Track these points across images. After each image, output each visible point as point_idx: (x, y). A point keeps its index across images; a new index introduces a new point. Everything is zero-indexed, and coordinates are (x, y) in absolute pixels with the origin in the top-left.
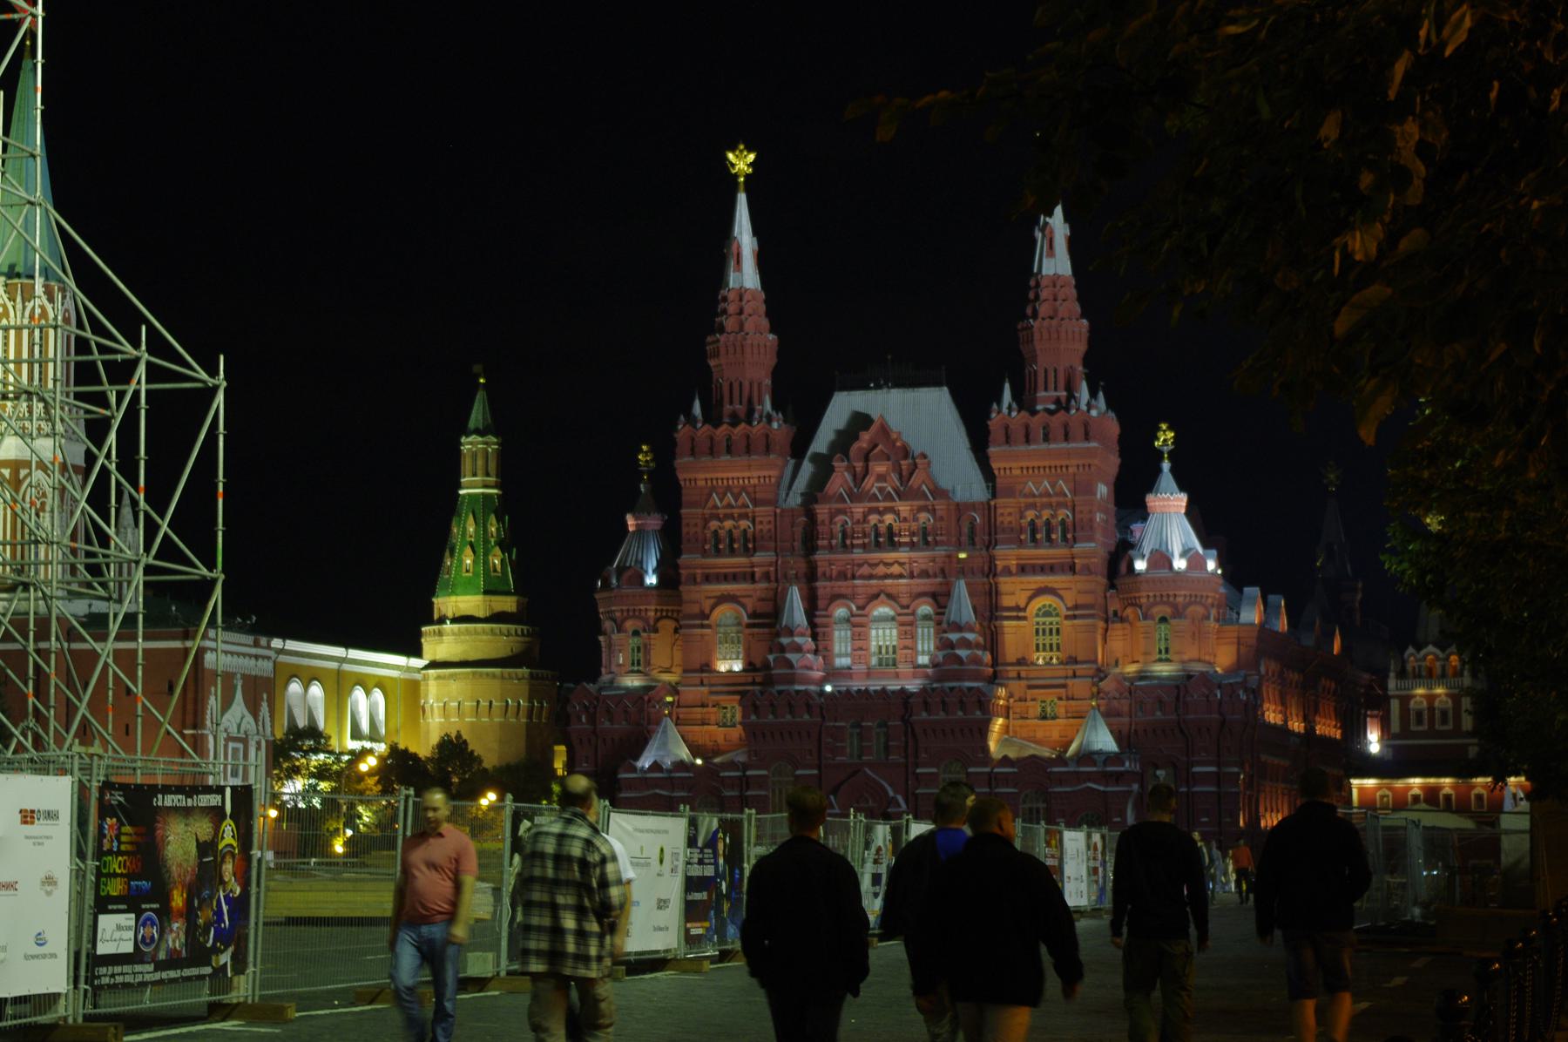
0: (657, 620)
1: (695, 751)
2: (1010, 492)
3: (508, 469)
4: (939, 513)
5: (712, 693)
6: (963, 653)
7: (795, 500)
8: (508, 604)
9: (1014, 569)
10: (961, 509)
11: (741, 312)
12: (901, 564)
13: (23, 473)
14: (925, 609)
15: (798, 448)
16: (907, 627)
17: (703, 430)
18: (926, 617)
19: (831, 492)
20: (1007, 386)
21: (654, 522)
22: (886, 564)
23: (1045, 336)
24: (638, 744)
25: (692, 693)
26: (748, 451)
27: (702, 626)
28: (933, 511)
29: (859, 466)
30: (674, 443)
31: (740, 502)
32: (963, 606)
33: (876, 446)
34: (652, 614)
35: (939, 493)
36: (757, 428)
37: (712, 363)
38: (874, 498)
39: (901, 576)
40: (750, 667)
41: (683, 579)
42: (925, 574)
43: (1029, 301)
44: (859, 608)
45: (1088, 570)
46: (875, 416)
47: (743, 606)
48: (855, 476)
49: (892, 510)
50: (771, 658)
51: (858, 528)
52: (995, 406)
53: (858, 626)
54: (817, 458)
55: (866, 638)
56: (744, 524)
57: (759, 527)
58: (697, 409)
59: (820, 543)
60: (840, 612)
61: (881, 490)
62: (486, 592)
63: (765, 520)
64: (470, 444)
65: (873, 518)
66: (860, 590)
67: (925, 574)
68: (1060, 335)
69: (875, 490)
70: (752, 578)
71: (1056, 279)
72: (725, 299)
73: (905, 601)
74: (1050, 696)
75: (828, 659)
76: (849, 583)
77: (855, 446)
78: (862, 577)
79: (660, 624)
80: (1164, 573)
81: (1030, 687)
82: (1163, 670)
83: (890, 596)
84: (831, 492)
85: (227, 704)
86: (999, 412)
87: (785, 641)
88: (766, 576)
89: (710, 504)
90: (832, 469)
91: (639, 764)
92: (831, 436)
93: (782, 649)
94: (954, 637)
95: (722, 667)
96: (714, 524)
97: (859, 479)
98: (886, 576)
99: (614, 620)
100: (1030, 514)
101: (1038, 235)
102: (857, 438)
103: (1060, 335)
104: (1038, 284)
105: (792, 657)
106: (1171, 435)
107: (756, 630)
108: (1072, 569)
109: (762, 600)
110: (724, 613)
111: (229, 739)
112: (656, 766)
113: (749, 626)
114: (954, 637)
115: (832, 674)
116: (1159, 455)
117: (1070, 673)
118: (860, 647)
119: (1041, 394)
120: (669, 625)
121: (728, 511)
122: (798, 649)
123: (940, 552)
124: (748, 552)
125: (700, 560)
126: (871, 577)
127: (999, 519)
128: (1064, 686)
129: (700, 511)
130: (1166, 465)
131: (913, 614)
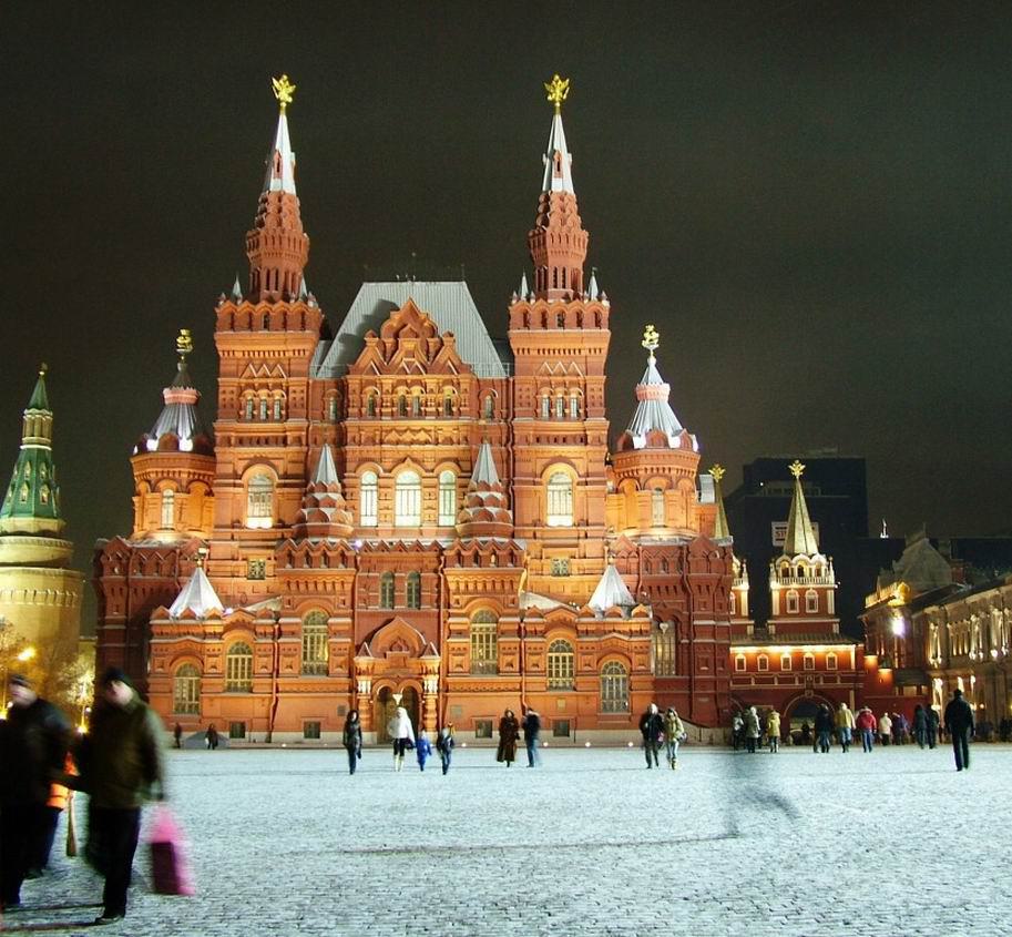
0: (190, 482)
1: (227, 600)
2: (528, 371)
3: (58, 433)
4: (463, 386)
5: (241, 547)
6: (493, 510)
7: (326, 374)
8: (51, 524)
9: (531, 439)
11: (280, 210)
12: (427, 431)
14: (448, 475)
15: (327, 334)
16: (430, 487)
17: (243, 307)
19: (362, 365)
20: (524, 278)
21: (188, 395)
22: (412, 431)
23: (556, 240)
24: (169, 596)
25: (223, 548)
26: (285, 326)
27: (235, 485)
29: (389, 341)
30: (215, 318)
31: (274, 373)
32: (487, 468)
33: (405, 325)
34: (185, 476)
36: (294, 306)
37: (250, 255)
39: (427, 442)
41: (218, 440)
42: (450, 441)
43: (539, 214)
44: (385, 471)
46: (402, 304)
48: (384, 353)
49: (420, 383)
50: (305, 511)
51: (388, 398)
52: (515, 294)
53: (384, 488)
54: (346, 339)
55: (393, 499)
56: (278, 393)
57: (292, 395)
58: (237, 289)
59: (350, 410)
61: (408, 364)
62: (36, 515)
63: (298, 389)
64: (30, 415)
65: (402, 390)
66: (388, 455)
67: (450, 441)
68: (567, 242)
69: (403, 364)
70: (285, 442)
72: (265, 201)
73: (430, 466)
74: (561, 556)
75: (357, 520)
76: (377, 447)
77: (386, 324)
78: (390, 443)
79: (191, 486)
80: (662, 451)
81: (544, 546)
82: (662, 536)
83: (415, 460)
84: (362, 365)
86: (519, 299)
87: (319, 496)
88: (298, 440)
89: (247, 374)
90: (364, 344)
91: (171, 611)
93: (316, 503)
94: (483, 495)
97: (388, 354)
98: (412, 443)
99: (149, 482)
101: (546, 161)
102: (388, 318)
103: (567, 242)
104: (547, 198)
105: (328, 511)
106: (656, 335)
107: (286, 490)
108: (584, 440)
109: (293, 462)
110: (257, 471)
112: (189, 615)
113: (279, 486)
114: (483, 495)
115: (360, 531)
117: (582, 535)
118: (386, 509)
119: (551, 290)
121: (263, 381)
122: (332, 504)
123: (464, 421)
126: (398, 443)
127: (517, 393)
128: (576, 546)
129: (237, 380)
130: (652, 361)
131: (437, 477)
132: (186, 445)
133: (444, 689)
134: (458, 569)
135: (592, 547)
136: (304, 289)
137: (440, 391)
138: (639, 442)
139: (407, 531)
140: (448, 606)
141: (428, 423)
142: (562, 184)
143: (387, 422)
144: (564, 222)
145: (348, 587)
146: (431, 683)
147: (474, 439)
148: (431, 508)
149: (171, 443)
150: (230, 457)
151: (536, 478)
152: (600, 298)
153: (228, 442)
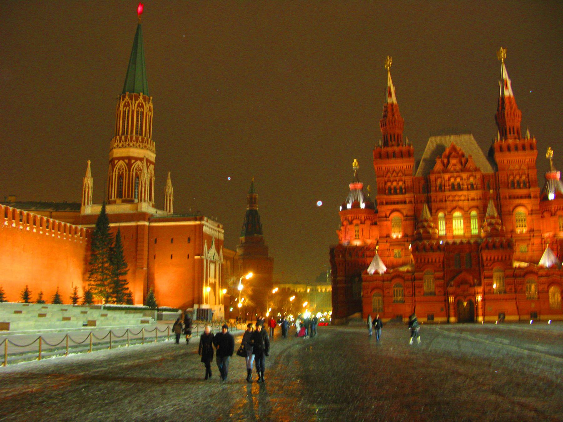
2: (503, 170)
10: (484, 178)
13: (133, 161)
16: (467, 220)
17: (384, 150)
18: (474, 216)
25: (384, 245)
28: (475, 177)
29: (445, 161)
32: (491, 209)
35: (477, 170)
38: (452, 172)
40: (405, 235)
42: (473, 199)
45: (535, 197)
47: (402, 213)
48: (444, 165)
49: (459, 176)
53: (448, 220)
54: (425, 160)
60: (441, 214)
67: (473, 199)
71: (509, 97)
85: (209, 248)
87: (426, 224)
88: (410, 202)
90: (435, 163)
92: (430, 152)
93: (423, 227)
94: (493, 221)
95: (394, 236)
96: (389, 184)
100: (511, 178)
108: (529, 197)
111: (211, 261)
112: (376, 273)
115: (440, 237)
116: (548, 160)
118: (449, 227)
119: (509, 136)
120: (368, 222)
122: (430, 227)
124: (401, 193)
125: (385, 197)
130: (551, 163)
132: (363, 206)
133: (484, 300)
134: (486, 251)
135: (537, 241)
136: (407, 141)
137: (468, 179)
138: (551, 196)
139: (458, 237)
140: (483, 266)
141: (465, 193)
142: (508, 93)
143: (447, 193)
144: (511, 108)
145: (441, 260)
146: (479, 298)
147: (485, 199)
148: (467, 226)
149: (356, 205)
150: (385, 210)
151: (511, 213)
152: (531, 138)
153: (382, 204)
